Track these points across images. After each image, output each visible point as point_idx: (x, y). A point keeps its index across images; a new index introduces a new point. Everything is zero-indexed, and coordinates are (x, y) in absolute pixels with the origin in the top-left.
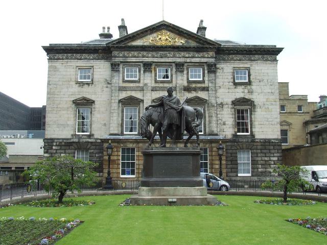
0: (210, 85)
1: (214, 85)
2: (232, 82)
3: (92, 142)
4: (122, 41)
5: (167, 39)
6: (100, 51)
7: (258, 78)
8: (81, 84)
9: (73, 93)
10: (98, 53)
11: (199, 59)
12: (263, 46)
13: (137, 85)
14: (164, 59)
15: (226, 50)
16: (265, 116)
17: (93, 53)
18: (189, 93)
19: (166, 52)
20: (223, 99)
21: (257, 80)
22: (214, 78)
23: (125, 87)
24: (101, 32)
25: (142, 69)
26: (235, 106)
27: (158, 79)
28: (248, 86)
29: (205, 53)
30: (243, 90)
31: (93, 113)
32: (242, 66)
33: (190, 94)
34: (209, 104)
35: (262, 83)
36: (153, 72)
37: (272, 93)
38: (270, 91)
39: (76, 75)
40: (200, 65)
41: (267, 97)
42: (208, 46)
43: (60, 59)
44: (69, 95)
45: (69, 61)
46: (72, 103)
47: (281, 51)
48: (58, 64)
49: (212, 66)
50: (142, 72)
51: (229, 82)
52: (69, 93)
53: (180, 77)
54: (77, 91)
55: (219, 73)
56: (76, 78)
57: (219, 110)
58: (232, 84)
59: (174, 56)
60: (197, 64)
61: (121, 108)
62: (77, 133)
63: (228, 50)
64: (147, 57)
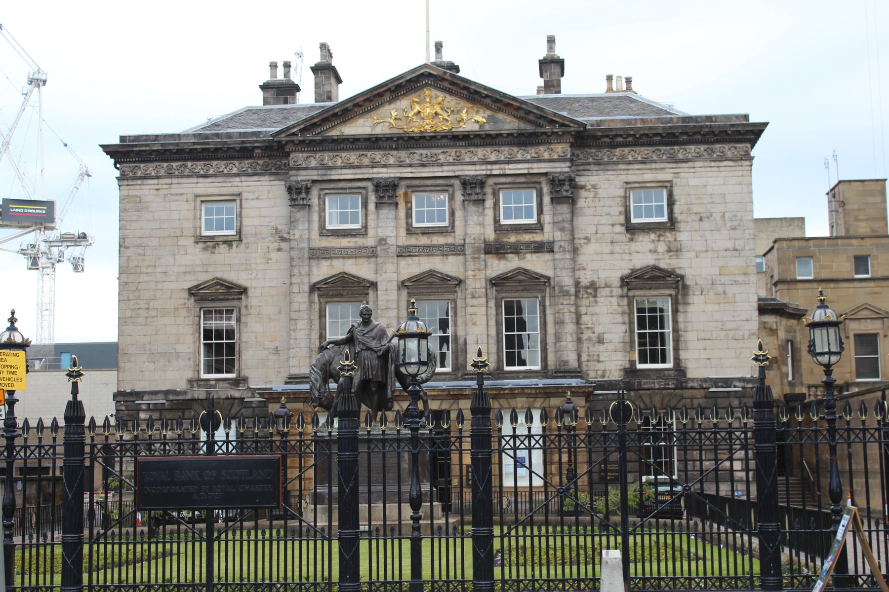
0: (558, 235)
1: (567, 237)
2: (622, 225)
4: (315, 125)
5: (436, 114)
6: (257, 151)
7: (696, 209)
8: (210, 243)
9: (188, 269)
10: (251, 157)
11: (526, 165)
12: (709, 118)
13: (360, 241)
14: (431, 169)
15: (602, 137)
17: (239, 158)
18: (500, 259)
19: (434, 151)
20: (595, 271)
21: (693, 217)
22: (568, 217)
23: (326, 249)
24: (265, 77)
25: (372, 198)
26: (629, 290)
27: (415, 225)
28: (668, 234)
29: (542, 148)
30: (652, 246)
31: (243, 319)
32: (648, 176)
33: (503, 262)
34: (554, 288)
35: (706, 224)
37: (735, 250)
38: (730, 244)
40: (530, 181)
42: (548, 128)
43: (152, 178)
44: (178, 273)
45: (175, 181)
46: (186, 295)
47: (761, 131)
48: (147, 192)
49: (561, 182)
50: (371, 206)
51: (613, 225)
52: (176, 269)
53: (476, 217)
54: (200, 263)
55: (585, 200)
56: (195, 228)
57: (584, 302)
58: (623, 229)
59: (458, 161)
60: (522, 180)
61: (316, 307)
62: (204, 376)
63: (607, 136)
64: (385, 166)
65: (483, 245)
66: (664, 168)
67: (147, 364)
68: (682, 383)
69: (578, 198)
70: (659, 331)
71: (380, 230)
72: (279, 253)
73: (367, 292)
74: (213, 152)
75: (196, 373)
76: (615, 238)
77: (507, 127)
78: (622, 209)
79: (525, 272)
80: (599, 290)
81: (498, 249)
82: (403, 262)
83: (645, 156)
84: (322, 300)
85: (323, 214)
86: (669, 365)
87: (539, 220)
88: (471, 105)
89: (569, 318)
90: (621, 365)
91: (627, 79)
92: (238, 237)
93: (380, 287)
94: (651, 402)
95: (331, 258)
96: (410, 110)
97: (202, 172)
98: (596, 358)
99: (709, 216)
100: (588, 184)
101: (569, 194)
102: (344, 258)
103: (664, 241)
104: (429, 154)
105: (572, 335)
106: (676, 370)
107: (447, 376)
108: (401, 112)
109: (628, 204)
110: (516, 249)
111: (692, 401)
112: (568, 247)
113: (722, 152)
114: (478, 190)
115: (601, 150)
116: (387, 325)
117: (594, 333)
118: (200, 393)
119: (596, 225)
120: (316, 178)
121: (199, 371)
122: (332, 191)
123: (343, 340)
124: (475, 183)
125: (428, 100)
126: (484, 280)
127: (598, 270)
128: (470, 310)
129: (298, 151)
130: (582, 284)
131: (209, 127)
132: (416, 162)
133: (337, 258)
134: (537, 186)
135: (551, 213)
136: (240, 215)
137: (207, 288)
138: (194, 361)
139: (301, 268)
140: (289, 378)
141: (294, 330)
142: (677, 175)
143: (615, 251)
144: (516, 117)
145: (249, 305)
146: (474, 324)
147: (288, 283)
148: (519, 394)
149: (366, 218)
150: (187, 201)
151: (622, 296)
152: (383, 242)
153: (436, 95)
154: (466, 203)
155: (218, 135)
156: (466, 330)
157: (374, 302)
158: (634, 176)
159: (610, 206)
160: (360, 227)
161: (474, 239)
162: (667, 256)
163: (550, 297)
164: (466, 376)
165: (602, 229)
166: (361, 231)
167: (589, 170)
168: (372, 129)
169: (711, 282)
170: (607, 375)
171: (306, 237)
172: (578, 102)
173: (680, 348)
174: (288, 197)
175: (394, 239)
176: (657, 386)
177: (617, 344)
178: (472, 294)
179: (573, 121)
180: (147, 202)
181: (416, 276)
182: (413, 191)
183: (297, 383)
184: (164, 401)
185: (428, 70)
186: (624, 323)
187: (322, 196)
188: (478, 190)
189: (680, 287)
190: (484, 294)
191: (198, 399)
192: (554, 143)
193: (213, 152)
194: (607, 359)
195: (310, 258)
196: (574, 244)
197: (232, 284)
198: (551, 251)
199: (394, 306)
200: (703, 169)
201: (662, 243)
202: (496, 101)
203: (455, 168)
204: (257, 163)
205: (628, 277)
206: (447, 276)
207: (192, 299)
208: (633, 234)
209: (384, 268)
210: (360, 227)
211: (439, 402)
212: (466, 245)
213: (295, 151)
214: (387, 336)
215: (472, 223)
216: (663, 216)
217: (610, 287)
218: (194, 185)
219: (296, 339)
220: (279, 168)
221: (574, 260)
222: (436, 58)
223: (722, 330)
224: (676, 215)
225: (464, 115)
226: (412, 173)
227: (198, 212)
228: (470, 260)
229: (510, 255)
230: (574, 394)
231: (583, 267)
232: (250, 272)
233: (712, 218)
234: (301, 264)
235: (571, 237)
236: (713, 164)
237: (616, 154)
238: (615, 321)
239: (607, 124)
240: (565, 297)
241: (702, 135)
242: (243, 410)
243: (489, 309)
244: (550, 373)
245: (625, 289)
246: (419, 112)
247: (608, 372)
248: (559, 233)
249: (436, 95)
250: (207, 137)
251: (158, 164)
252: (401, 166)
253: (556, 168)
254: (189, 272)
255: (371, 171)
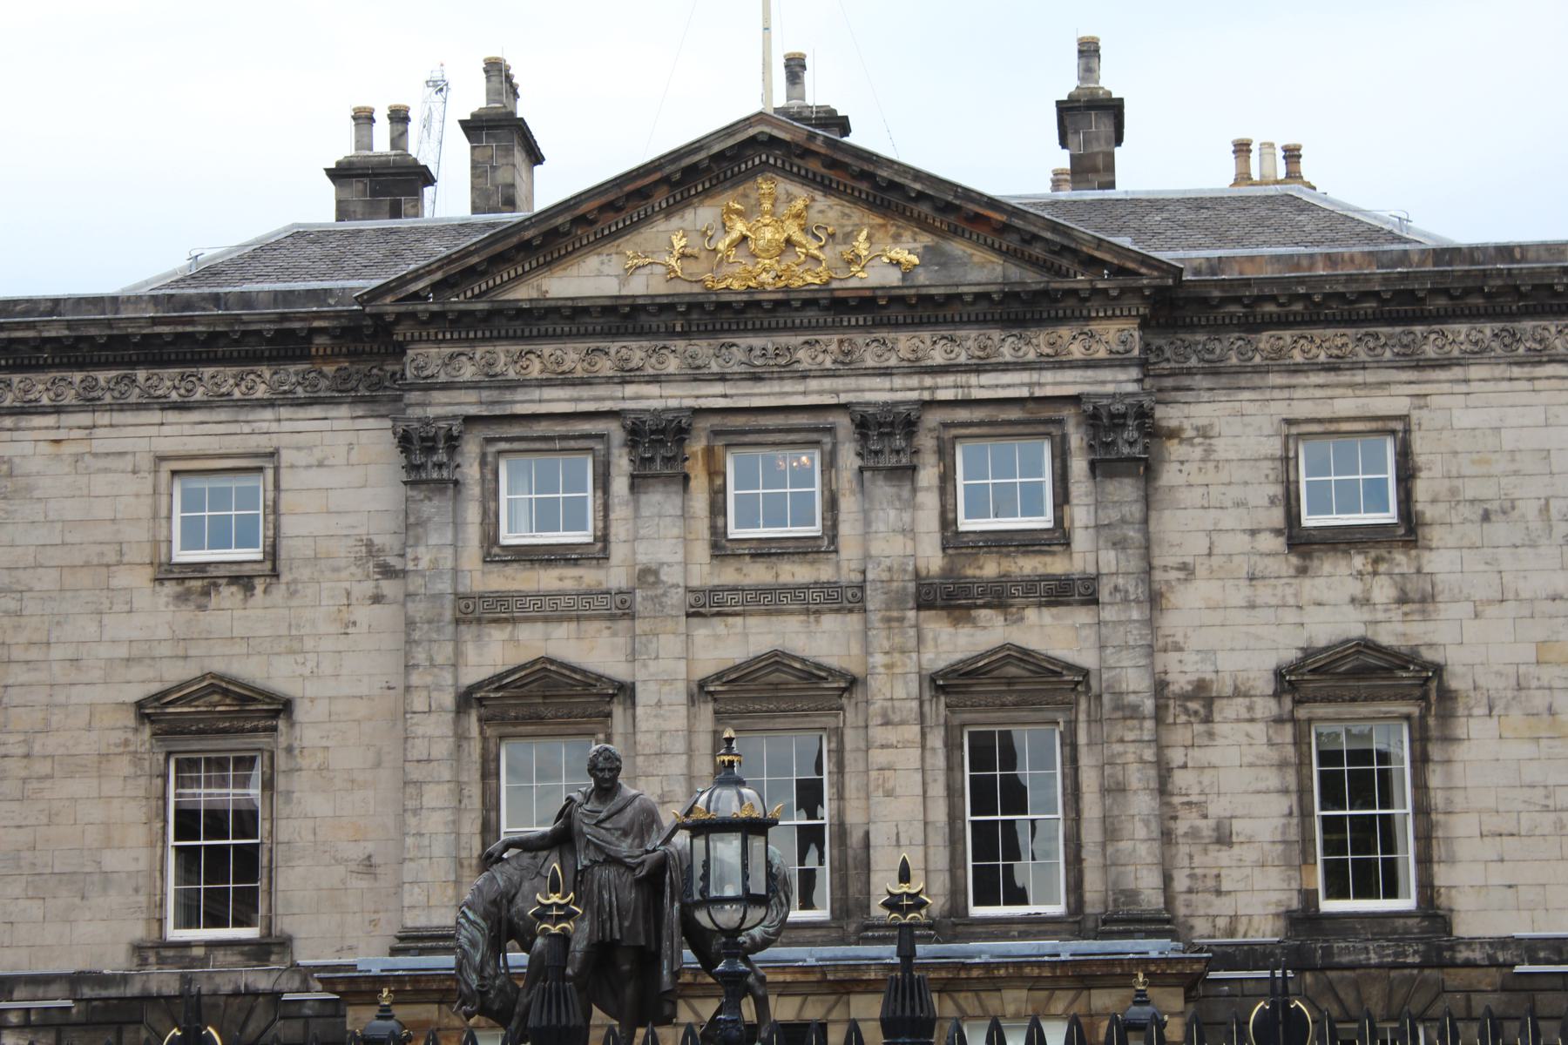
0: (1109, 559)
1: (1134, 563)
2: (1278, 532)
3: (275, 996)
4: (471, 273)
5: (789, 242)
6: (320, 340)
7: (1471, 490)
9: (136, 652)
11: (1025, 377)
12: (1505, 252)
13: (589, 576)
14: (776, 387)
15: (1224, 301)
16: (1532, 773)
17: (274, 359)
18: (956, 622)
19: (784, 340)
20: (1208, 653)
21: (1465, 511)
22: (1136, 511)
23: (501, 598)
24: (343, 147)
25: (622, 464)
26: (1297, 702)
27: (734, 532)
28: (1399, 557)
29: (1065, 332)
30: (1356, 588)
31: (281, 782)
32: (1346, 405)
34: (1099, 697)
35: (1499, 530)
36: (699, 483)
39: (159, 516)
41: (1539, 631)
42: (1081, 280)
44: (111, 660)
45: (103, 418)
46: (131, 721)
48: (28, 448)
49: (1117, 421)
50: (620, 485)
52: (104, 651)
53: (892, 513)
54: (163, 632)
56: (155, 543)
57: (1180, 735)
58: (1279, 543)
59: (847, 366)
60: (1014, 414)
61: (474, 749)
62: (175, 934)
63: (1237, 300)
64: (655, 379)
65: (911, 587)
66: (1388, 383)
67: (23, 903)
68: (1440, 949)
69: (1162, 461)
70: (1377, 811)
71: (641, 547)
72: (376, 606)
73: (607, 709)
74: (205, 343)
75: (156, 926)
76: (1260, 567)
77: (975, 275)
78: (1278, 490)
79: (1024, 656)
80: (1218, 704)
81: (951, 596)
82: (702, 631)
83: (1335, 352)
84: (489, 732)
85: (492, 505)
86: (1406, 903)
87: (1059, 520)
88: (879, 221)
89: (1138, 778)
90: (1279, 903)
91: (1286, 149)
92: (268, 566)
93: (642, 696)
94: (1360, 1000)
95: (513, 621)
96: (720, 233)
97: (174, 396)
98: (1211, 883)
99: (1508, 508)
100: (1186, 424)
101: (1137, 451)
102: (546, 620)
103: (1390, 574)
104: (770, 346)
105: (1147, 823)
106: (1425, 917)
107: (818, 932)
108: (696, 239)
109: (1292, 477)
110: (999, 595)
111: (1468, 1000)
112: (1135, 590)
113: (1540, 341)
114: (899, 442)
115: (1222, 336)
116: (662, 796)
117: (1205, 817)
118: (164, 981)
119: (1209, 533)
120: (473, 411)
121: (161, 922)
122: (516, 446)
123: (543, 836)
124: (892, 424)
125: (767, 205)
126: (914, 678)
127: (1215, 652)
128: (878, 757)
129: (428, 340)
130: (1174, 688)
131: (193, 277)
132: (736, 369)
133: (527, 620)
134: (1054, 430)
135: (1091, 500)
136: (275, 509)
137: (187, 700)
138: (151, 895)
139: (435, 647)
140: (401, 939)
141: (415, 812)
142: (1422, 402)
143: (1259, 601)
144: (999, 251)
145: (296, 744)
146: (889, 794)
147: (399, 682)
148: (1009, 978)
149: (606, 516)
150: (134, 472)
151: (1279, 720)
152: (651, 579)
153: (788, 194)
154: (867, 474)
155: (216, 299)
156: (868, 808)
157: (625, 735)
158: (1309, 404)
159: (1246, 483)
160: (591, 540)
161: (890, 569)
162: (1396, 613)
163: (1089, 722)
164: (868, 932)
165: (1225, 544)
166: (591, 549)
167: (1189, 389)
168: (622, 284)
169: (1513, 682)
170: (1241, 929)
171: (449, 564)
172: (1161, 210)
173: (1435, 858)
174: (402, 460)
175: (678, 569)
176: (1374, 959)
177: (1267, 847)
178: (884, 714)
179: (1146, 260)
180: (28, 475)
181: (736, 668)
182: (727, 446)
183: (422, 952)
184: (69, 1003)
185: (767, 129)
186: (1285, 791)
187: (490, 459)
188: (899, 442)
189: (1433, 696)
190: (914, 715)
191: (160, 997)
192: (1097, 317)
193: (205, 343)
194: (1241, 886)
195: (457, 622)
196: (1150, 582)
197: (252, 689)
198: (1092, 600)
199: (680, 746)
200: (1490, 386)
201: (1383, 580)
202: (946, 208)
203: (839, 383)
204: (320, 373)
205: (1294, 668)
206: (819, 666)
207: (147, 731)
208: (1306, 556)
209: (653, 646)
210: (591, 540)
211: (797, 1000)
212: (869, 587)
213: (420, 340)
214: (661, 828)
215: (882, 527)
216: (1386, 510)
217: (1246, 695)
218: (154, 430)
219: (422, 835)
220: (378, 385)
221: (1151, 624)
222: (789, 98)
223: (1546, 808)
224: (1419, 507)
225: (862, 246)
226: (725, 396)
227: (164, 500)
228: (877, 625)
229: (984, 613)
230: (1154, 979)
231: (1176, 643)
232: (300, 658)
233: (1515, 514)
234: (434, 636)
235: (1143, 564)
236: (1516, 371)
237: (1262, 346)
238: (1262, 786)
239: (1236, 267)
240: (1130, 723)
241: (1489, 296)
242: (279, 1024)
243: (928, 754)
244: (1090, 924)
245: (1288, 702)
246: (744, 238)
247: (1244, 920)
248: (1112, 554)
249: (787, 192)
250: (188, 303)
251: (59, 375)
252: (696, 380)
253: (1104, 383)
254: (140, 660)
255: (618, 391)
